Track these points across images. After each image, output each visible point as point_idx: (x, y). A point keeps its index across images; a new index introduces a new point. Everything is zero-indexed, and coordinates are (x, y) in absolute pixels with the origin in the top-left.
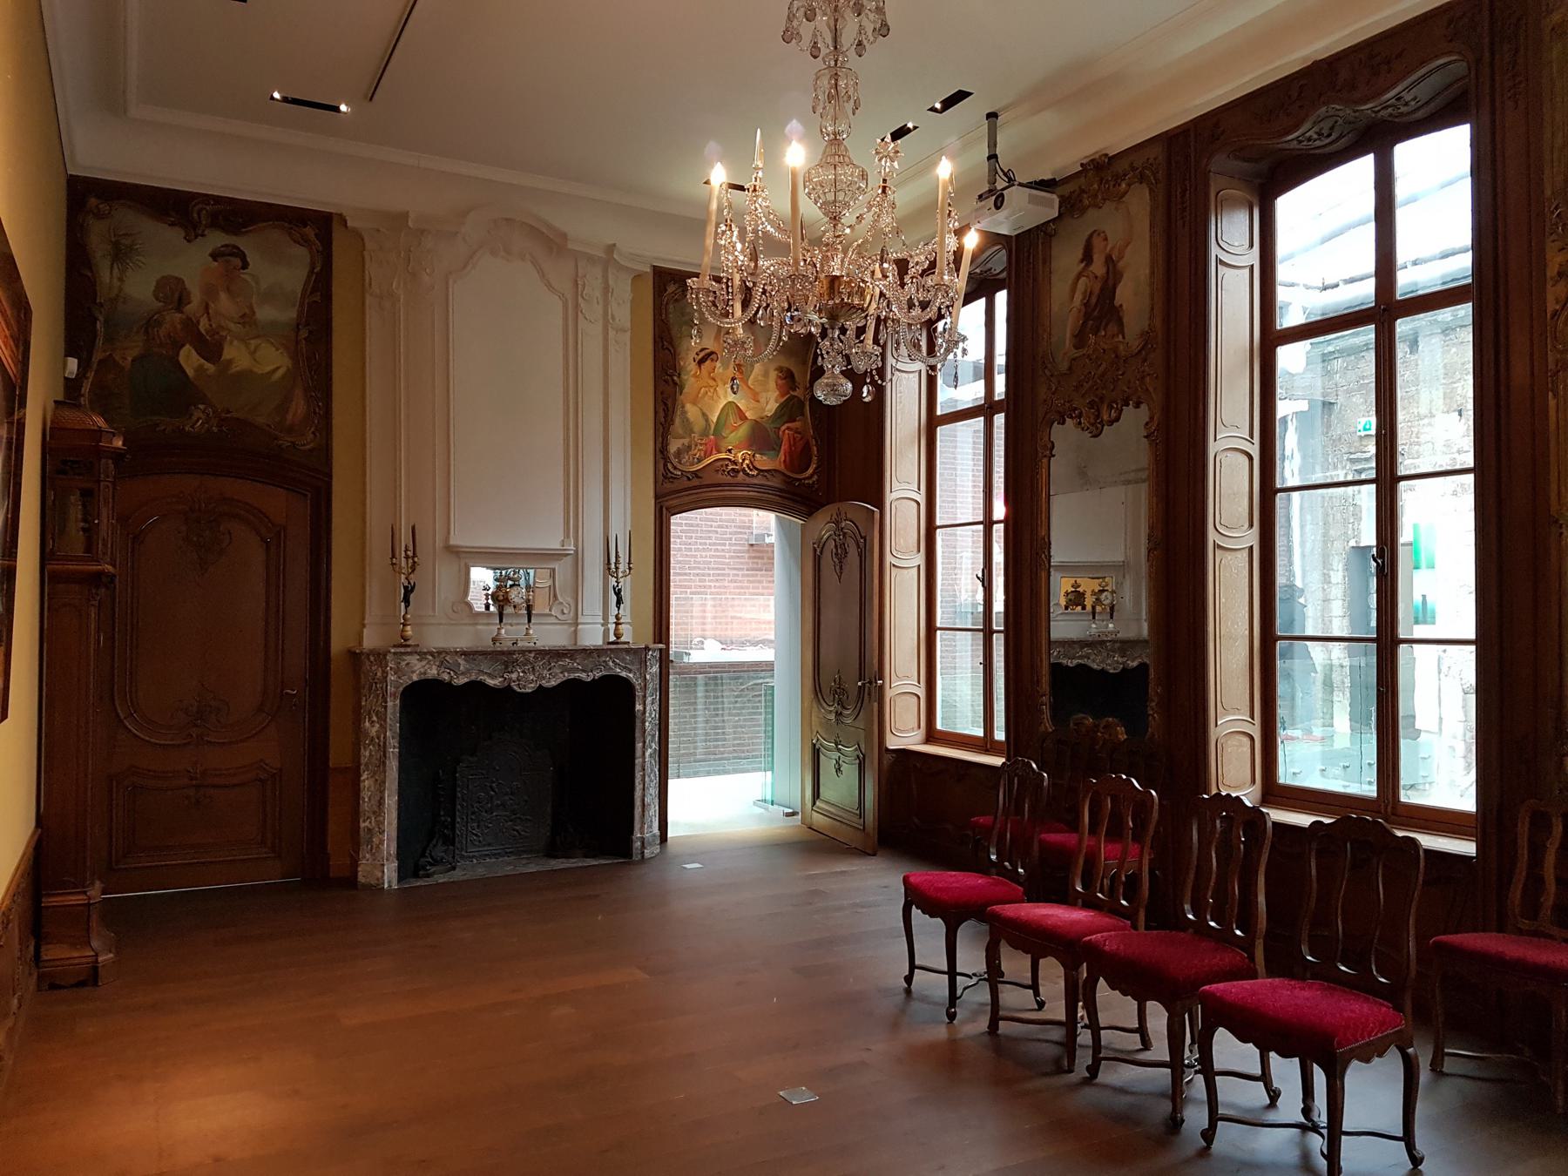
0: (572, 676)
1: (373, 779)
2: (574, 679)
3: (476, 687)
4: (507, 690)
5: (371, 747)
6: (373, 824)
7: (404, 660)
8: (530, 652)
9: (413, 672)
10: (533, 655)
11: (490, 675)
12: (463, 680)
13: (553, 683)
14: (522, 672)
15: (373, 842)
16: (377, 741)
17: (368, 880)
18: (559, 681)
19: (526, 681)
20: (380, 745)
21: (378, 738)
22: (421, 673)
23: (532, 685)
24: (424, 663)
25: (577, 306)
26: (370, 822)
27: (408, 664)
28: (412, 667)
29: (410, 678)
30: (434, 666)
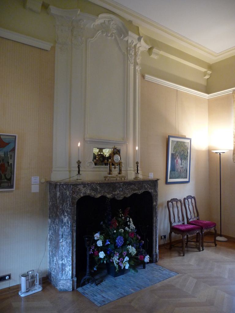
0: (136, 192)
1: (66, 241)
2: (135, 194)
3: (103, 198)
4: (113, 200)
5: (64, 227)
6: (66, 261)
7: (78, 187)
8: (121, 182)
9: (81, 193)
10: (122, 184)
11: (108, 193)
12: (99, 196)
13: (129, 195)
14: (119, 191)
15: (65, 270)
16: (67, 224)
17: (64, 288)
18: (131, 194)
19: (120, 194)
20: (68, 226)
21: (68, 223)
22: (84, 193)
23: (122, 197)
24: (85, 188)
25: (128, 57)
26: (64, 261)
27: (79, 189)
28: (81, 191)
29: (80, 196)
30: (88, 190)
